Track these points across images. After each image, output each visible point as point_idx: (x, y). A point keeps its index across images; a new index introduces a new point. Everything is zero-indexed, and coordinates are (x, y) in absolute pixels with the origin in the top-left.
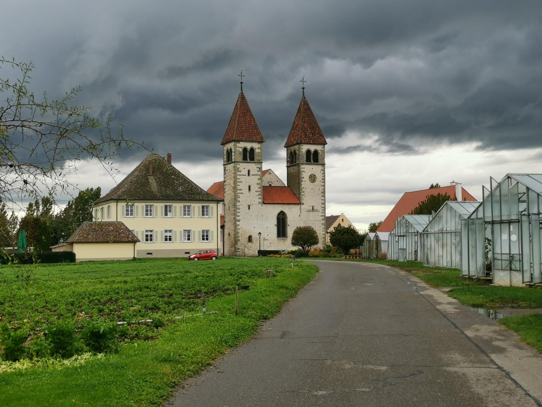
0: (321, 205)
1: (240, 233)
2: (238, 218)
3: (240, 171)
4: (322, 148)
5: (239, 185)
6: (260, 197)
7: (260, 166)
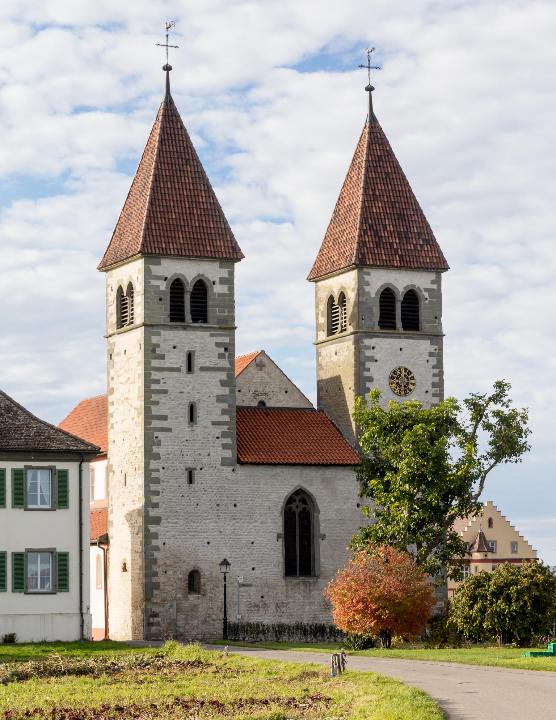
7: (227, 340)
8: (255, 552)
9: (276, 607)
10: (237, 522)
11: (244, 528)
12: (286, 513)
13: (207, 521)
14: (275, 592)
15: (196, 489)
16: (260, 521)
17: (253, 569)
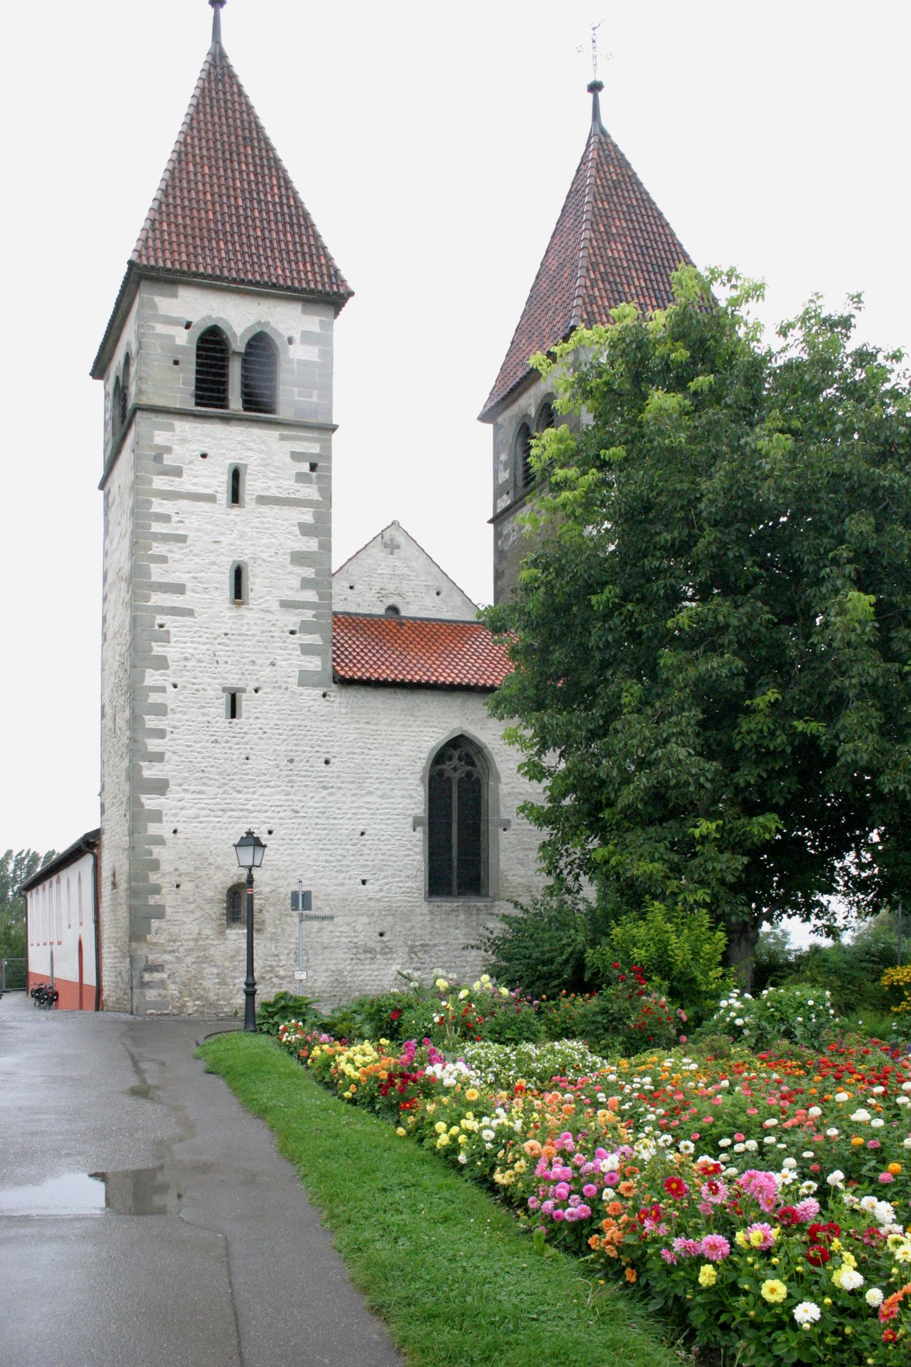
2: (150, 771)
3: (177, 472)
5: (163, 559)
6: (314, 639)
7: (314, 448)
8: (366, 851)
9: (410, 952)
10: (330, 794)
11: (345, 806)
12: (432, 779)
13: (267, 791)
14: (408, 925)
15: (245, 730)
16: (379, 793)
17: (364, 882)
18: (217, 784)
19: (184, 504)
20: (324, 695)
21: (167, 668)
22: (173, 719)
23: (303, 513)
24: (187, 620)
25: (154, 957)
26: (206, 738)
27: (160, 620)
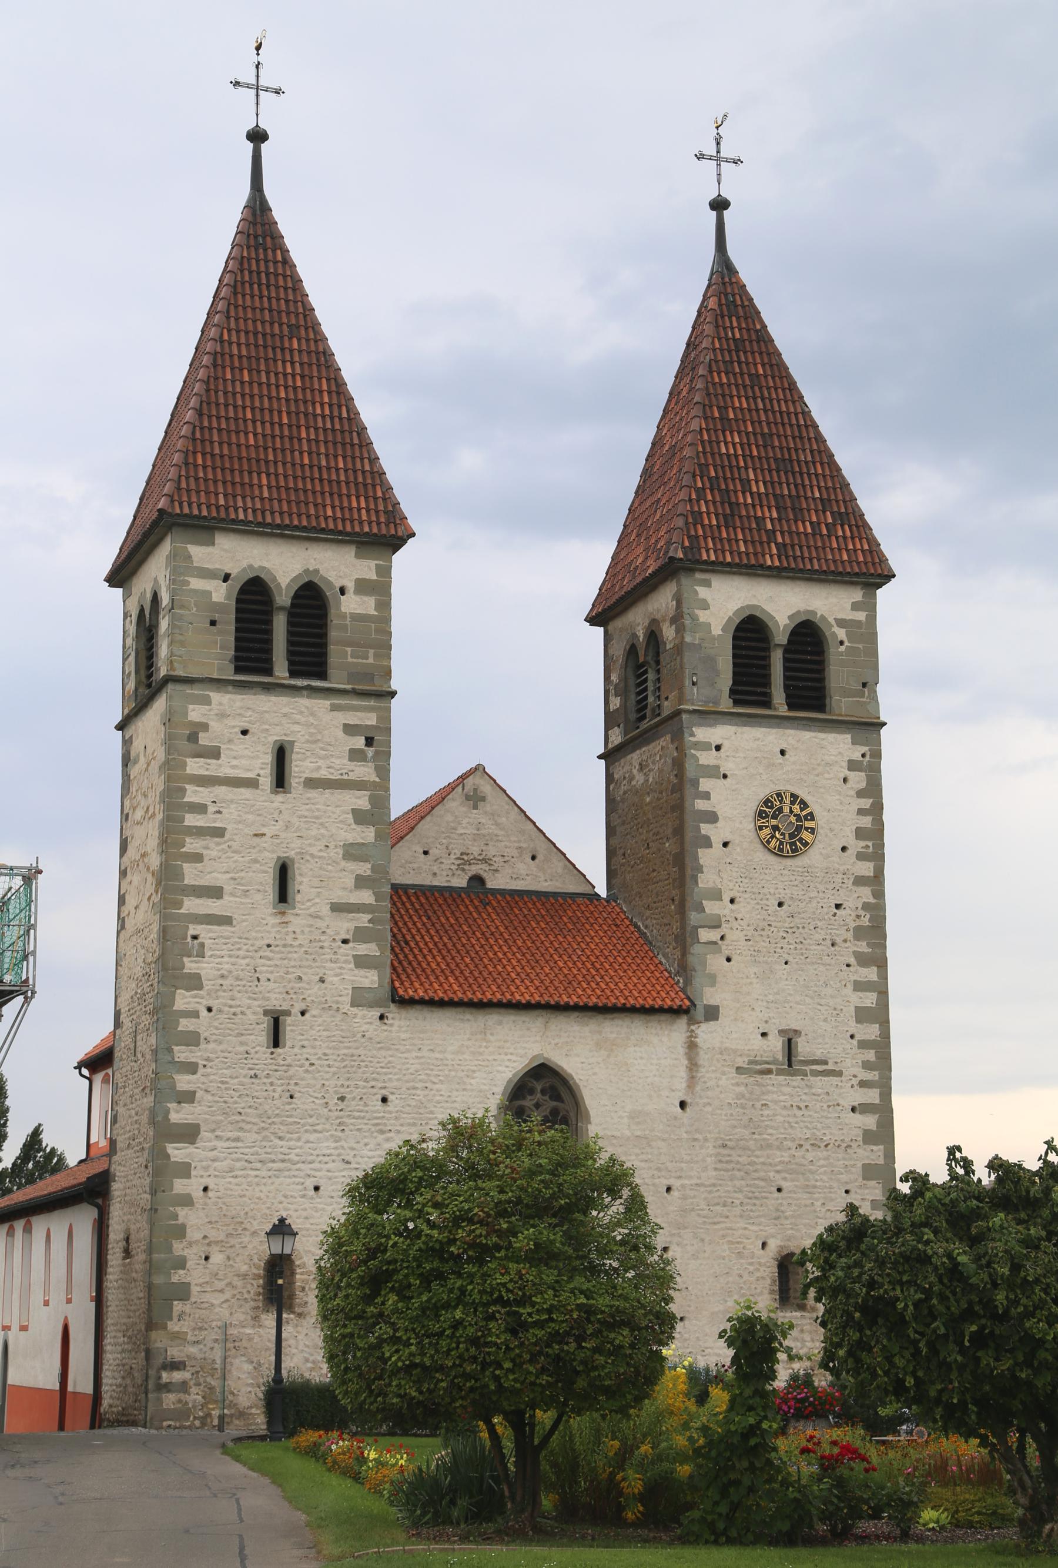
0: (853, 1027)
1: (193, 1234)
2: (178, 1115)
3: (214, 753)
4: (855, 607)
5: (197, 858)
6: (370, 949)
13: (313, 1137)
18: (255, 1128)
19: (222, 791)
20: (382, 1017)
21: (200, 987)
22: (206, 1050)
23: (359, 798)
24: (225, 930)
25: (175, 1353)
26: (244, 1072)
27: (193, 930)
